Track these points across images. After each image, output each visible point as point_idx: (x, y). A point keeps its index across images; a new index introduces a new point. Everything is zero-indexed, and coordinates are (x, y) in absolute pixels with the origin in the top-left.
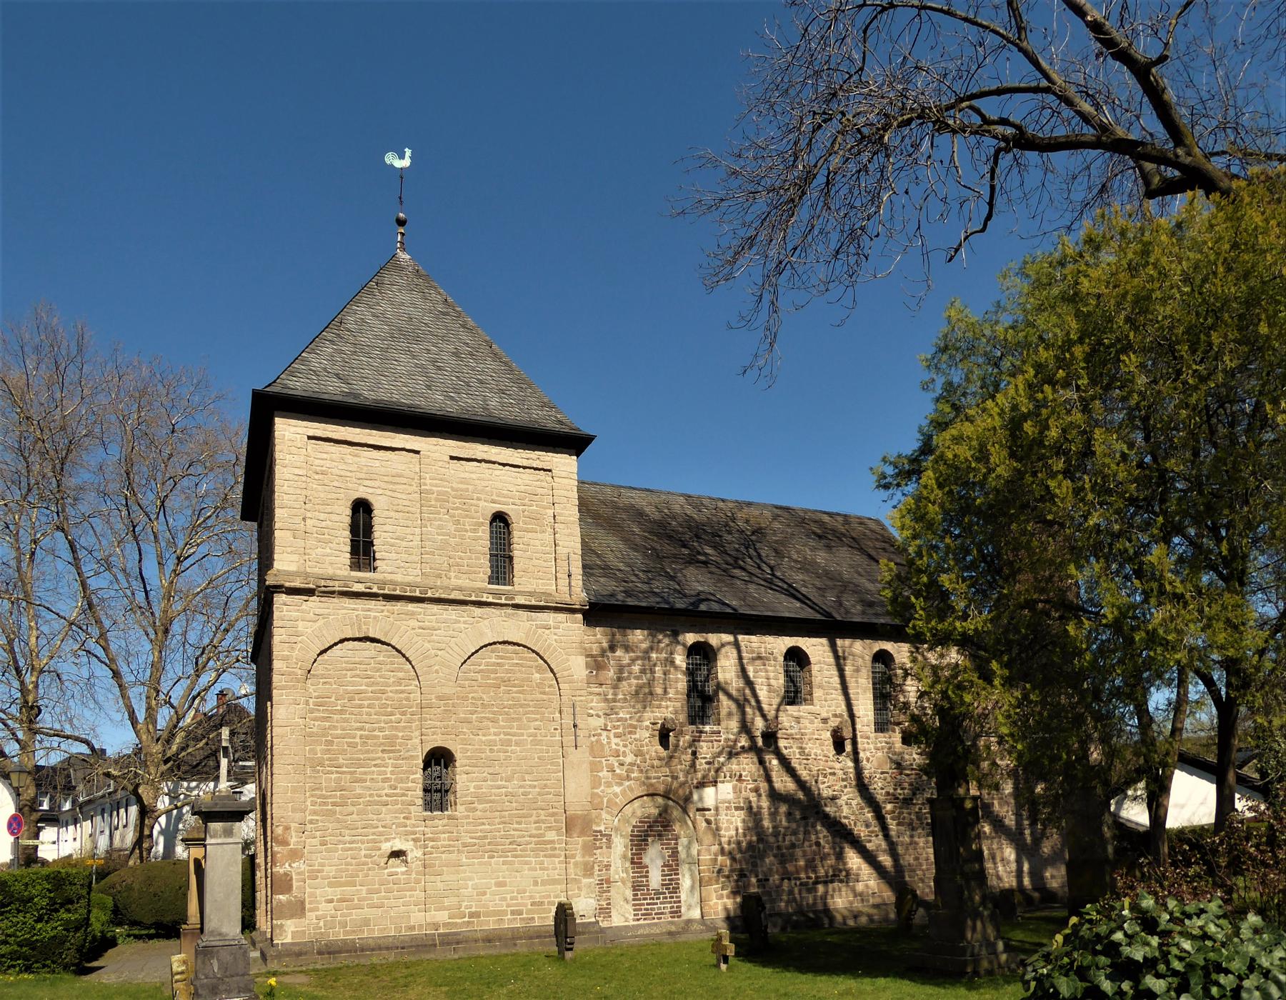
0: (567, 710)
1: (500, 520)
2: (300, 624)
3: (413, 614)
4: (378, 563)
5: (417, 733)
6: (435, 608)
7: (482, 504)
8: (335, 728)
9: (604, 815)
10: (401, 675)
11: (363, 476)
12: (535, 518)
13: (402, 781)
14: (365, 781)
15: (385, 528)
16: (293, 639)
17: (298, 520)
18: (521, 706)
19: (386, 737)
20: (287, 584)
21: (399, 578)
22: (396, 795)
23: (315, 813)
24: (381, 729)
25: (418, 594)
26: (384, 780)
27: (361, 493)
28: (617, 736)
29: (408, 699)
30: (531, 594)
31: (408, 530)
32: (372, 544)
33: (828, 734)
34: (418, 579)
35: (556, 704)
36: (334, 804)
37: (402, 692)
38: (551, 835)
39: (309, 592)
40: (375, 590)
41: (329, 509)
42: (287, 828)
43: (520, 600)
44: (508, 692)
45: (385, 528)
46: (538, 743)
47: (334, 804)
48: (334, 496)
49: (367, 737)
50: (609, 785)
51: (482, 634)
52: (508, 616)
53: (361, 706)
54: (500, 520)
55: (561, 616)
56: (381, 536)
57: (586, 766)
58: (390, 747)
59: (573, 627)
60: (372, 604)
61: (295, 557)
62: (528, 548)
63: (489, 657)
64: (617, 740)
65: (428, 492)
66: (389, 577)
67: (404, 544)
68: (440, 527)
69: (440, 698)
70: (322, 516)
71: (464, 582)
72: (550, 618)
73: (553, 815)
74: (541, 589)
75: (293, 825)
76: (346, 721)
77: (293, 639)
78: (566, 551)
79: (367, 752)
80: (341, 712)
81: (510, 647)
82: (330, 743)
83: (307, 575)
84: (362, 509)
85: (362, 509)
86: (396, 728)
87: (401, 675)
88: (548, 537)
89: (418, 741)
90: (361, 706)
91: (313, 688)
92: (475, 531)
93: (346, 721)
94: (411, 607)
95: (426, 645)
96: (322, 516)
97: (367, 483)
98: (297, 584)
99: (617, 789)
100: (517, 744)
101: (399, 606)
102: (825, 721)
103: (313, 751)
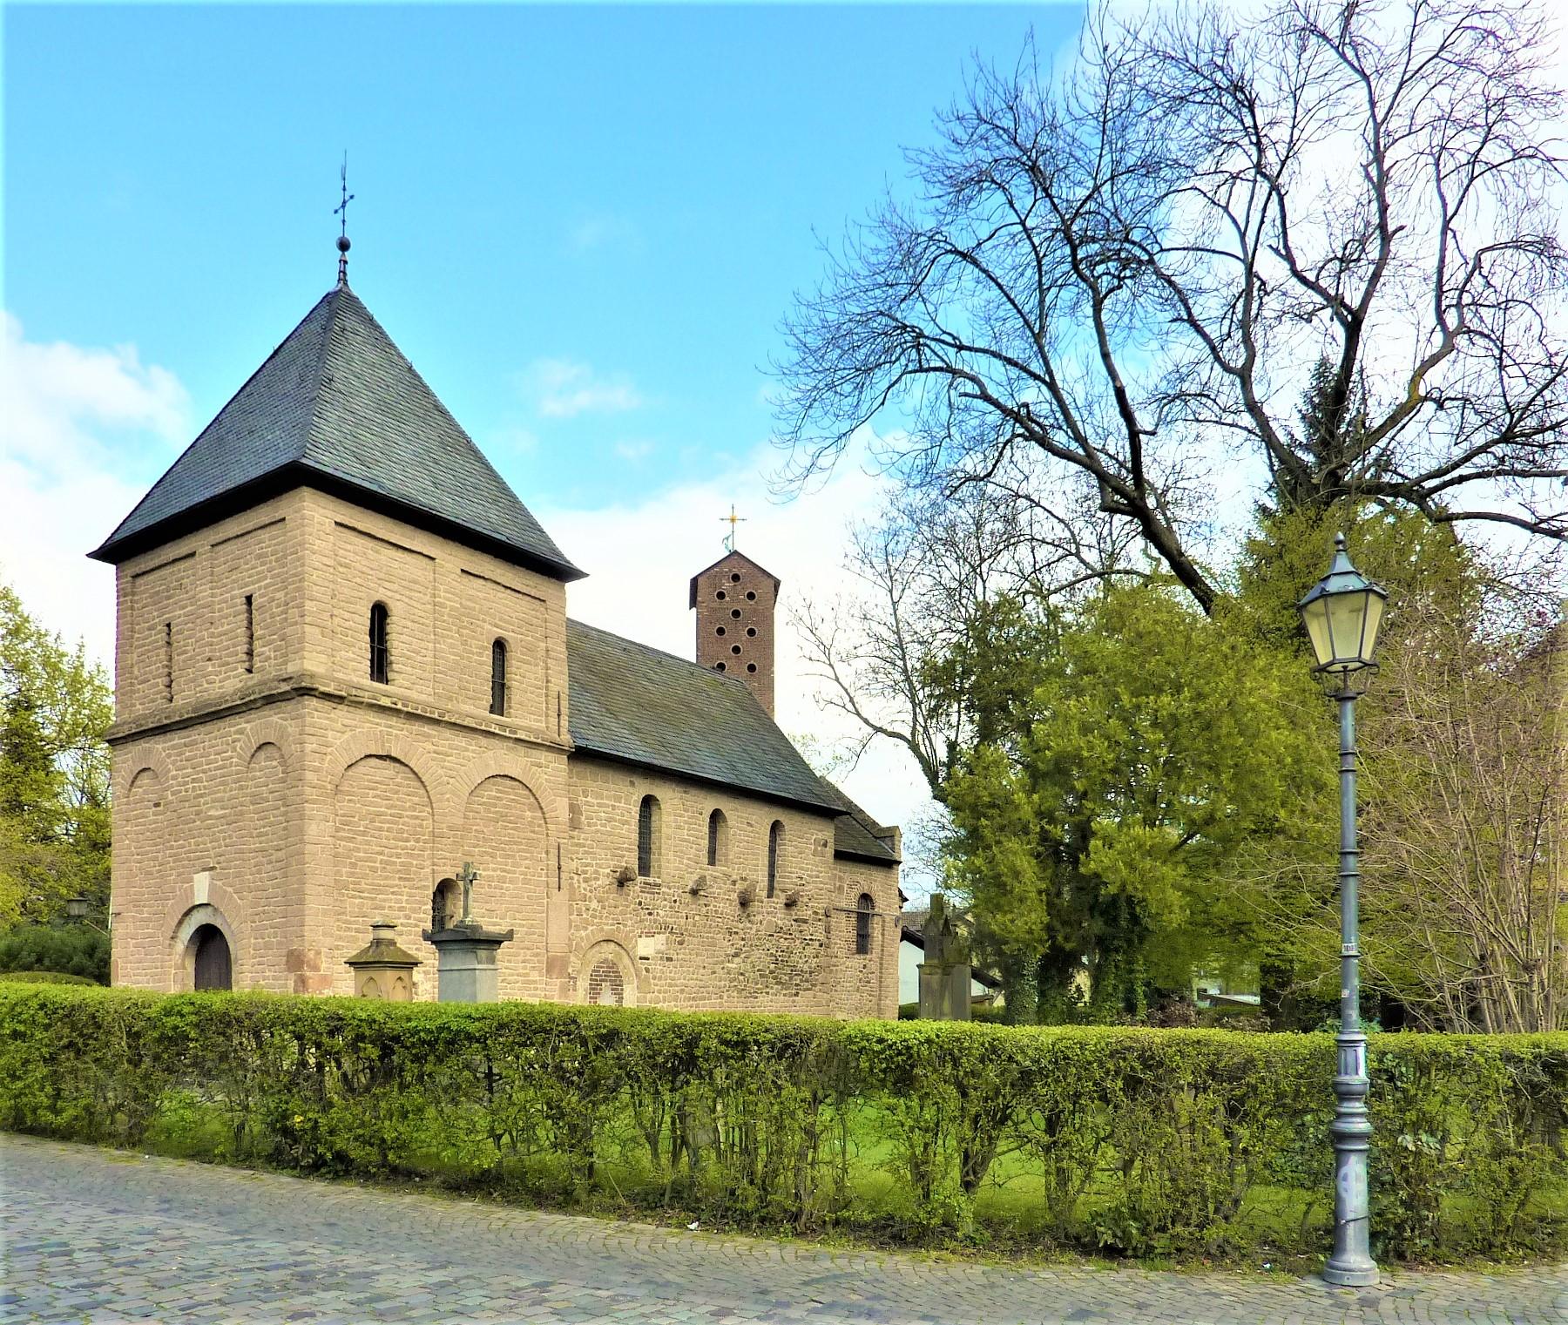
0: (554, 852)
1: (500, 646)
2: (330, 733)
3: (429, 736)
4: (391, 676)
5: (428, 863)
6: (447, 733)
7: (487, 626)
8: (358, 850)
9: (572, 959)
10: (416, 799)
11: (381, 575)
12: (531, 650)
13: (414, 911)
14: (383, 908)
15: (403, 638)
16: (323, 749)
17: (326, 616)
18: (515, 843)
19: (402, 864)
20: (322, 689)
21: (414, 695)
22: (409, 925)
23: (341, 938)
24: (398, 856)
25: (436, 716)
26: (401, 909)
27: (381, 595)
28: (586, 881)
29: (421, 826)
30: (529, 730)
31: (423, 644)
32: (386, 650)
33: (734, 896)
34: (431, 699)
35: (543, 844)
36: (357, 931)
37: (417, 818)
38: (534, 976)
39: (340, 699)
40: (399, 706)
41: (352, 607)
42: (318, 953)
43: (521, 735)
44: (505, 828)
45: (403, 638)
46: (526, 881)
47: (357, 931)
48: (356, 594)
49: (387, 863)
50: (577, 929)
51: (487, 765)
52: (509, 749)
53: (380, 829)
54: (500, 646)
55: (551, 756)
56: (398, 643)
57: (565, 909)
58: (406, 875)
59: (560, 764)
60: (393, 721)
61: (323, 658)
62: (520, 674)
63: (491, 791)
64: (583, 885)
65: (442, 605)
66: (407, 693)
67: (419, 658)
68: (452, 646)
69: (450, 829)
70: (347, 616)
71: (467, 708)
72: (543, 757)
73: (537, 955)
74: (535, 725)
75: (324, 950)
76: (368, 843)
77: (323, 749)
78: (557, 688)
79: (386, 878)
80: (364, 833)
81: (508, 782)
82: (353, 865)
83: (339, 681)
84: (380, 613)
85: (380, 613)
86: (411, 856)
87: (416, 799)
88: (541, 672)
89: (428, 870)
90: (380, 829)
91: (344, 806)
92: (480, 654)
93: (368, 843)
94: (427, 729)
95: (440, 771)
96: (347, 616)
97: (387, 585)
98: (330, 689)
99: (583, 933)
100: (511, 882)
101: (417, 727)
102: (734, 882)
103: (338, 873)
